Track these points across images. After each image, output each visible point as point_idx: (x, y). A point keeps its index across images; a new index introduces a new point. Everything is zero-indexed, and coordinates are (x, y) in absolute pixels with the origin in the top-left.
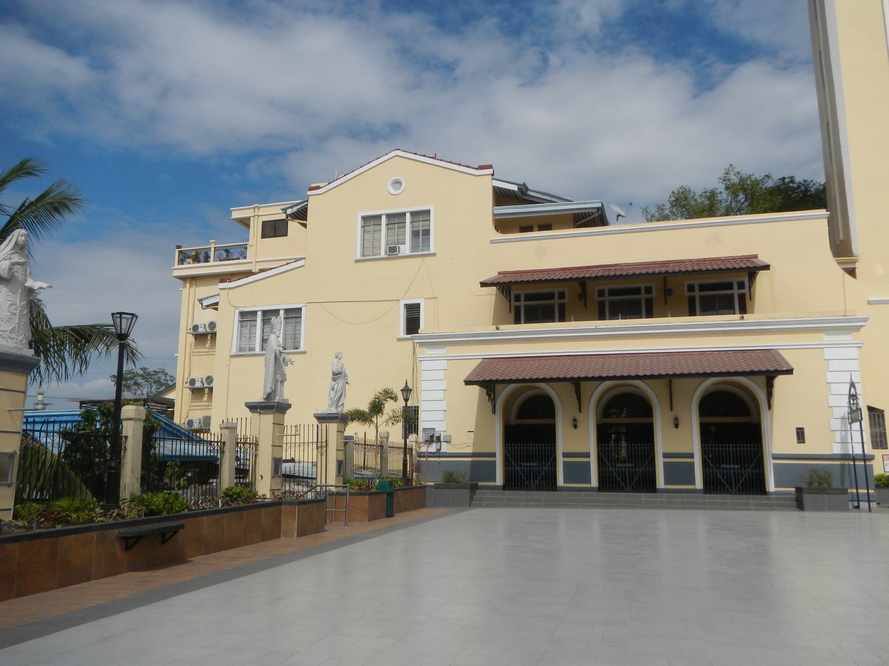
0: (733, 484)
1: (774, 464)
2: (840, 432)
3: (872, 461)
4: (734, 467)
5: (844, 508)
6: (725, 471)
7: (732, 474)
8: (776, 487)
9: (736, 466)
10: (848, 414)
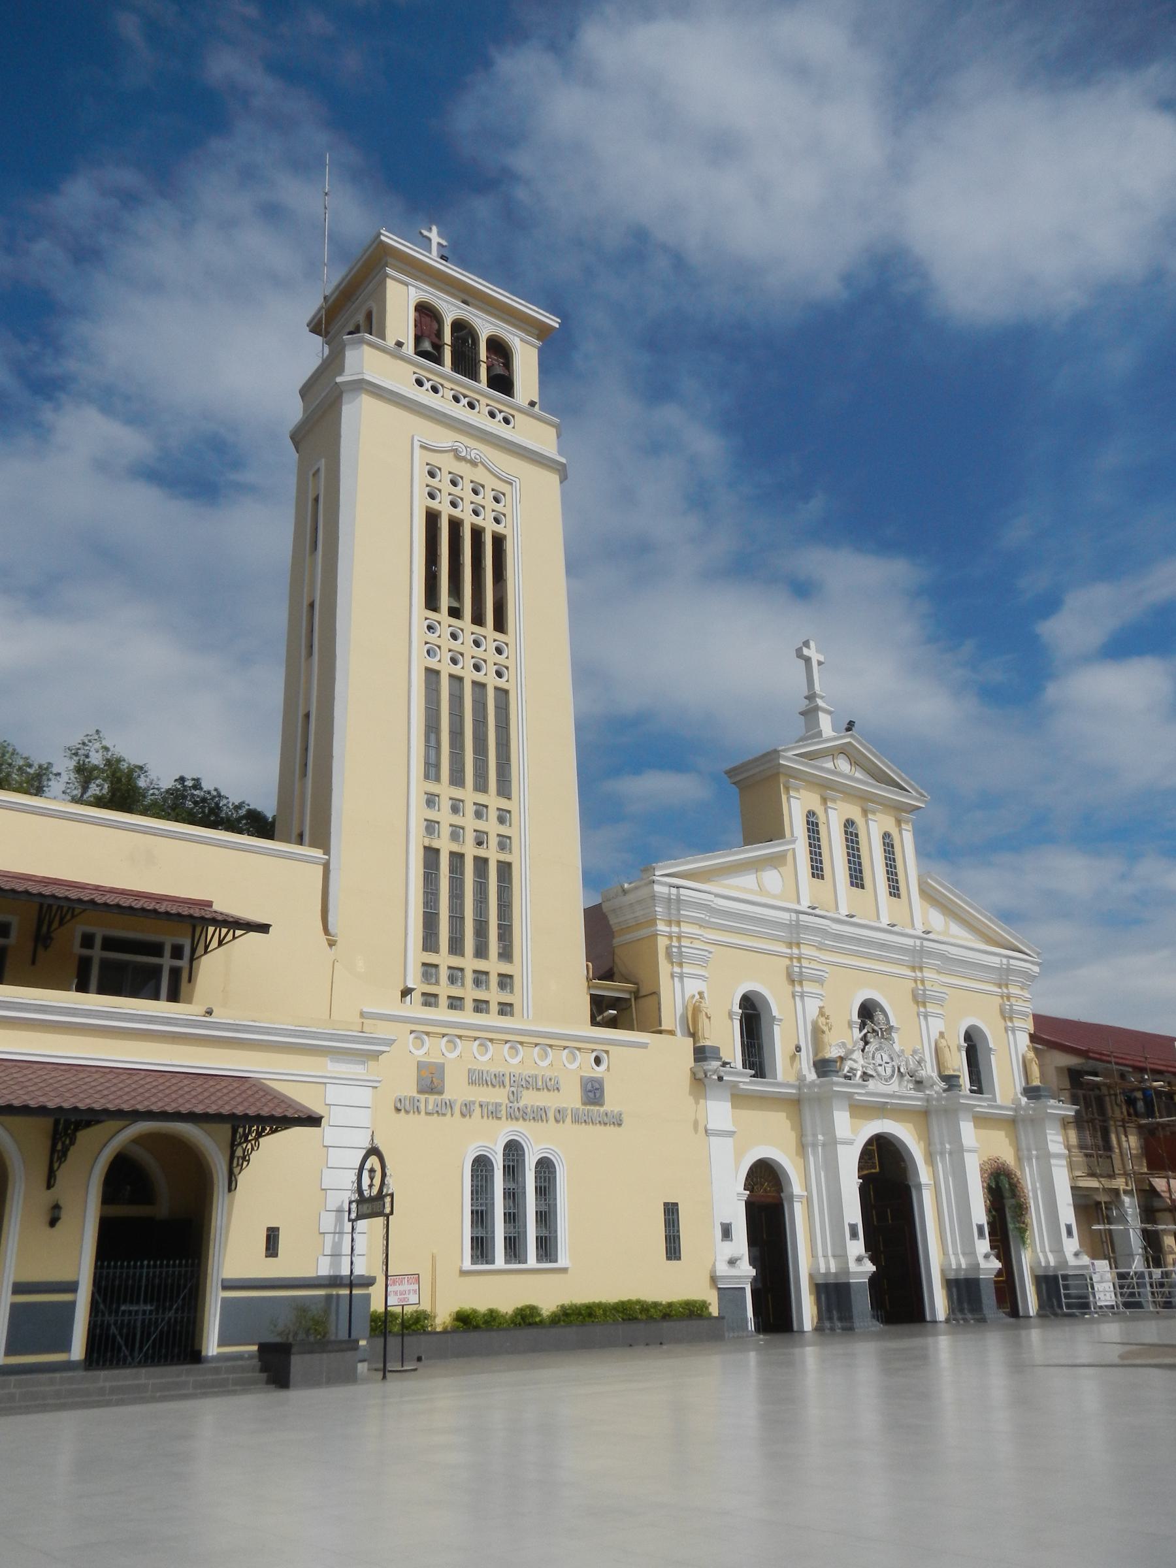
0: (137, 1345)
1: (224, 1300)
2: (332, 1235)
3: (370, 1288)
4: (145, 1308)
5: (349, 1377)
6: (126, 1318)
7: (139, 1324)
8: (219, 1345)
9: (149, 1308)
10: (350, 1203)
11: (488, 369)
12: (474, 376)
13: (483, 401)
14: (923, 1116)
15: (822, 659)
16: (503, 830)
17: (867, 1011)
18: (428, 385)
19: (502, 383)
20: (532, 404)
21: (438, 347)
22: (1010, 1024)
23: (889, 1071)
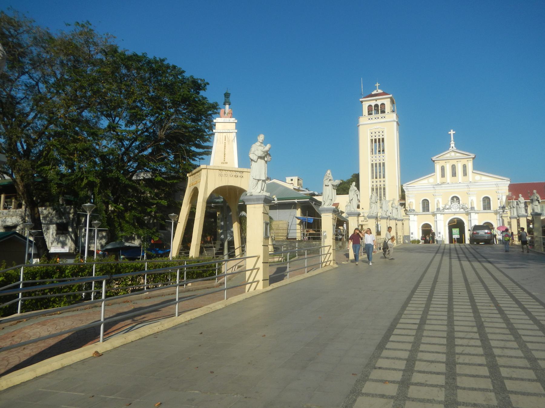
11: (381, 110)
12: (379, 114)
13: (380, 116)
14: (468, 214)
15: (454, 132)
16: (384, 183)
17: (453, 198)
18: (370, 119)
19: (383, 112)
20: (388, 113)
21: (372, 111)
22: (498, 195)
23: (457, 207)
